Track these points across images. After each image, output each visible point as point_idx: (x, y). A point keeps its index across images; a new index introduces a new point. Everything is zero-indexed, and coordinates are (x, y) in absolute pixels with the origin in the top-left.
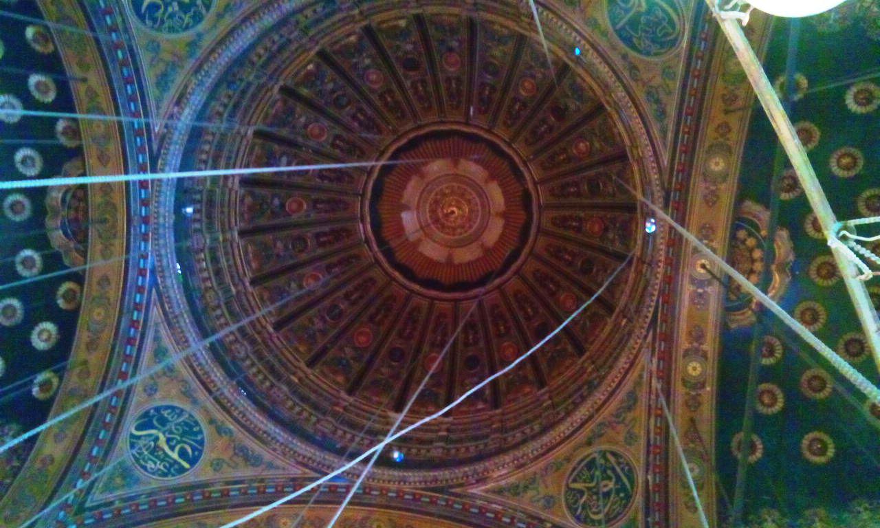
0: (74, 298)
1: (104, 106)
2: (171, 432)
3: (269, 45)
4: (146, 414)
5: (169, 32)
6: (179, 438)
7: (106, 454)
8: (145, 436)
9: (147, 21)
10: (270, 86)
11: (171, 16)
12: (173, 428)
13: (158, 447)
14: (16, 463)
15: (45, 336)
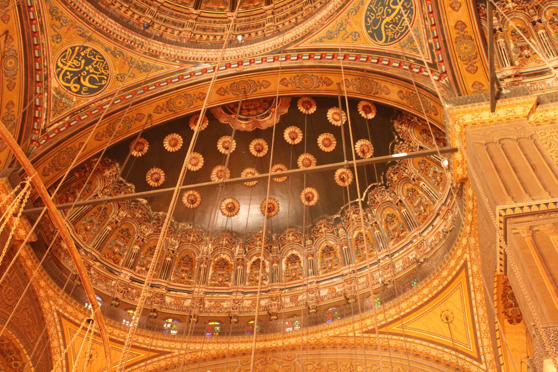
0: (308, 102)
1: (164, 101)
2: (383, 14)
3: (124, 9)
4: (371, 35)
5: (108, 69)
6: (387, 7)
7: (398, 56)
8: (385, 32)
9: (103, 83)
10: (160, 5)
11: (96, 69)
12: (379, 14)
13: (392, 20)
14: (416, 119)
15: (337, 117)
